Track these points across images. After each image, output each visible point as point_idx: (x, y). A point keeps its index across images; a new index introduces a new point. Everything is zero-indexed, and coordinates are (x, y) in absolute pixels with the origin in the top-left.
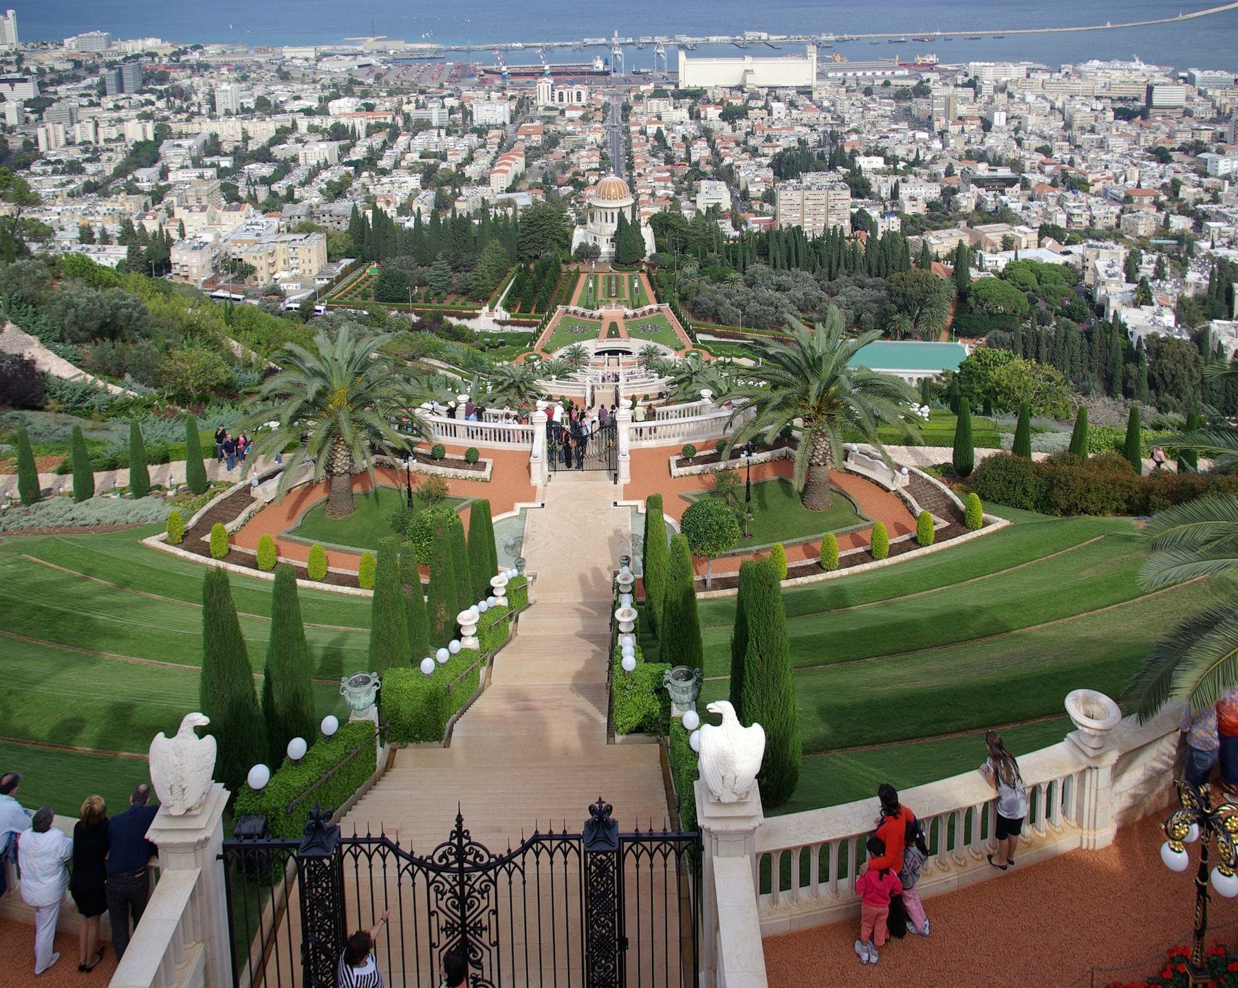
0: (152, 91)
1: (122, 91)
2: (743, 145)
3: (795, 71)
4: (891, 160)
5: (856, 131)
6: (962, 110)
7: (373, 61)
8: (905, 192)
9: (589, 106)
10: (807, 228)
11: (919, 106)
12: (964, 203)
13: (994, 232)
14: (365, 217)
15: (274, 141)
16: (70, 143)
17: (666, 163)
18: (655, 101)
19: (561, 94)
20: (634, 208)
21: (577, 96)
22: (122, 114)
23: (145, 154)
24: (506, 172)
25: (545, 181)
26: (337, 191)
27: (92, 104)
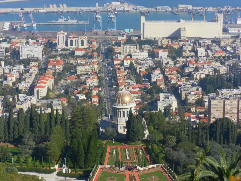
3: (210, 30)
9: (89, 48)
18: (128, 46)
19: (72, 41)
21: (81, 44)
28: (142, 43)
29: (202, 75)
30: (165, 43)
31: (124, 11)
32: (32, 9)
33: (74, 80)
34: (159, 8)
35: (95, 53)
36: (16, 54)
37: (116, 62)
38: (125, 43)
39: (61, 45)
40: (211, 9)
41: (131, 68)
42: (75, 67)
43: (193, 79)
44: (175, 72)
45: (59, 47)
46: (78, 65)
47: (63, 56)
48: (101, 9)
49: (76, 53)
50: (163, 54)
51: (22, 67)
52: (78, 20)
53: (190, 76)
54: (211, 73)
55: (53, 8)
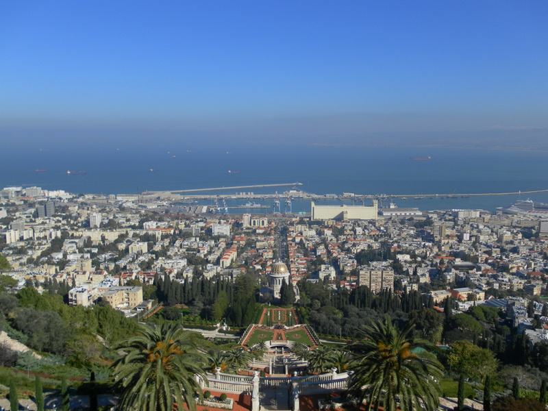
0: (60, 216)
1: (46, 216)
2: (342, 247)
3: (367, 213)
4: (413, 256)
5: (396, 242)
6: (448, 232)
7: (165, 204)
8: (420, 272)
9: (268, 228)
10: (373, 288)
11: (428, 229)
12: (449, 277)
13: (463, 293)
14: (161, 279)
15: (117, 241)
16: (21, 239)
17: (305, 256)
18: (300, 226)
19: (254, 221)
20: (290, 277)
21: (262, 223)
22: (46, 226)
23: (57, 245)
24: (227, 259)
25: (246, 263)
26: (146, 266)
27: (31, 221)
28: (311, 223)
29: (359, 249)
30: (330, 223)
31: (299, 198)
32: (226, 196)
33: (254, 253)
34: (328, 195)
35: (273, 232)
36: (209, 231)
37: (289, 239)
38: (298, 224)
39: (246, 224)
40: (370, 196)
41: (301, 242)
42: (255, 243)
43: (351, 253)
44: (336, 248)
45: (244, 226)
46: (258, 241)
47: (247, 234)
48: (281, 196)
49: (258, 231)
50: (328, 233)
51: (213, 242)
52: (262, 205)
53: (348, 251)
54: (366, 248)
55: (243, 195)
